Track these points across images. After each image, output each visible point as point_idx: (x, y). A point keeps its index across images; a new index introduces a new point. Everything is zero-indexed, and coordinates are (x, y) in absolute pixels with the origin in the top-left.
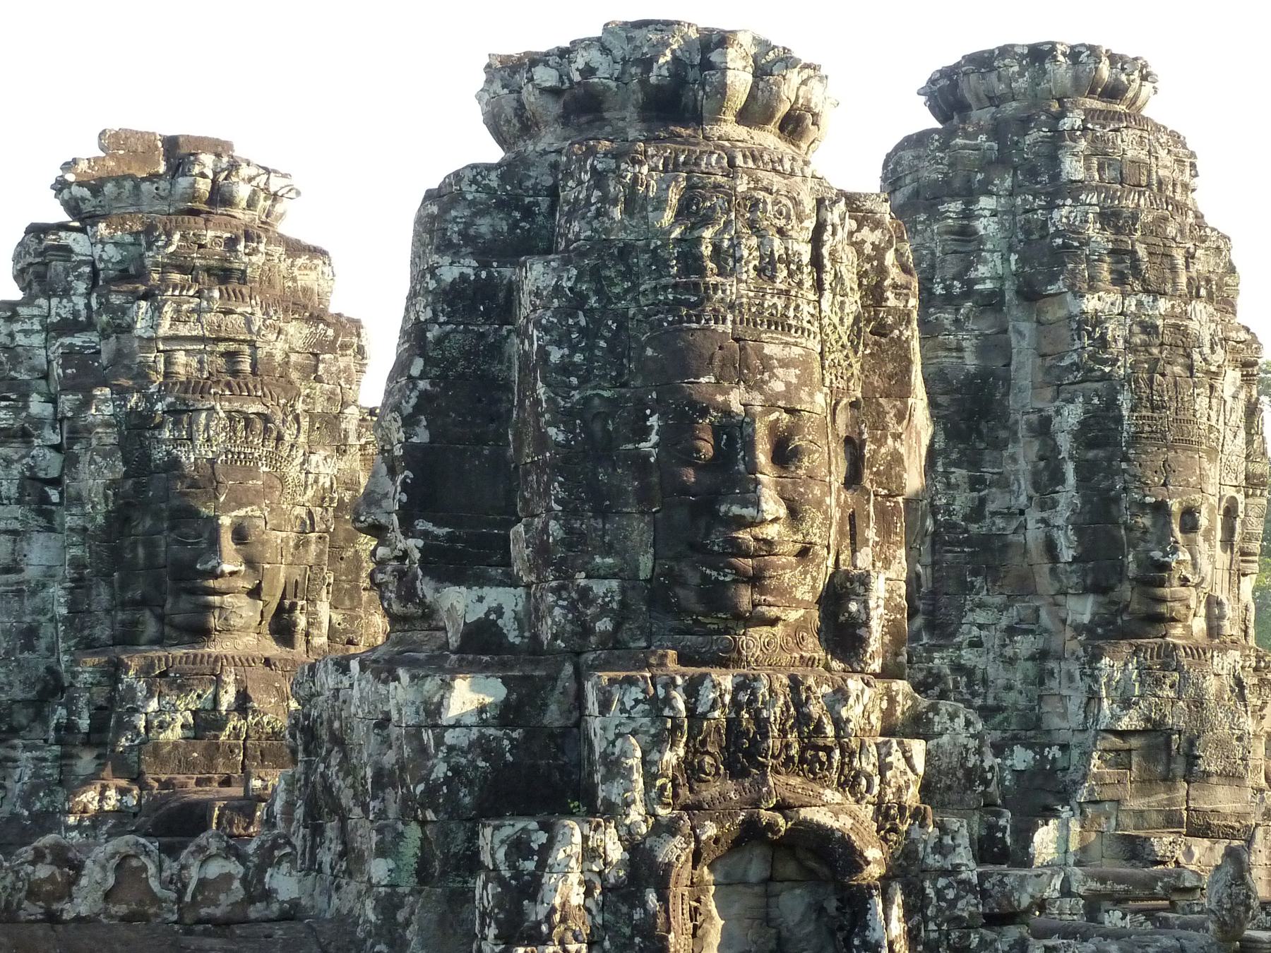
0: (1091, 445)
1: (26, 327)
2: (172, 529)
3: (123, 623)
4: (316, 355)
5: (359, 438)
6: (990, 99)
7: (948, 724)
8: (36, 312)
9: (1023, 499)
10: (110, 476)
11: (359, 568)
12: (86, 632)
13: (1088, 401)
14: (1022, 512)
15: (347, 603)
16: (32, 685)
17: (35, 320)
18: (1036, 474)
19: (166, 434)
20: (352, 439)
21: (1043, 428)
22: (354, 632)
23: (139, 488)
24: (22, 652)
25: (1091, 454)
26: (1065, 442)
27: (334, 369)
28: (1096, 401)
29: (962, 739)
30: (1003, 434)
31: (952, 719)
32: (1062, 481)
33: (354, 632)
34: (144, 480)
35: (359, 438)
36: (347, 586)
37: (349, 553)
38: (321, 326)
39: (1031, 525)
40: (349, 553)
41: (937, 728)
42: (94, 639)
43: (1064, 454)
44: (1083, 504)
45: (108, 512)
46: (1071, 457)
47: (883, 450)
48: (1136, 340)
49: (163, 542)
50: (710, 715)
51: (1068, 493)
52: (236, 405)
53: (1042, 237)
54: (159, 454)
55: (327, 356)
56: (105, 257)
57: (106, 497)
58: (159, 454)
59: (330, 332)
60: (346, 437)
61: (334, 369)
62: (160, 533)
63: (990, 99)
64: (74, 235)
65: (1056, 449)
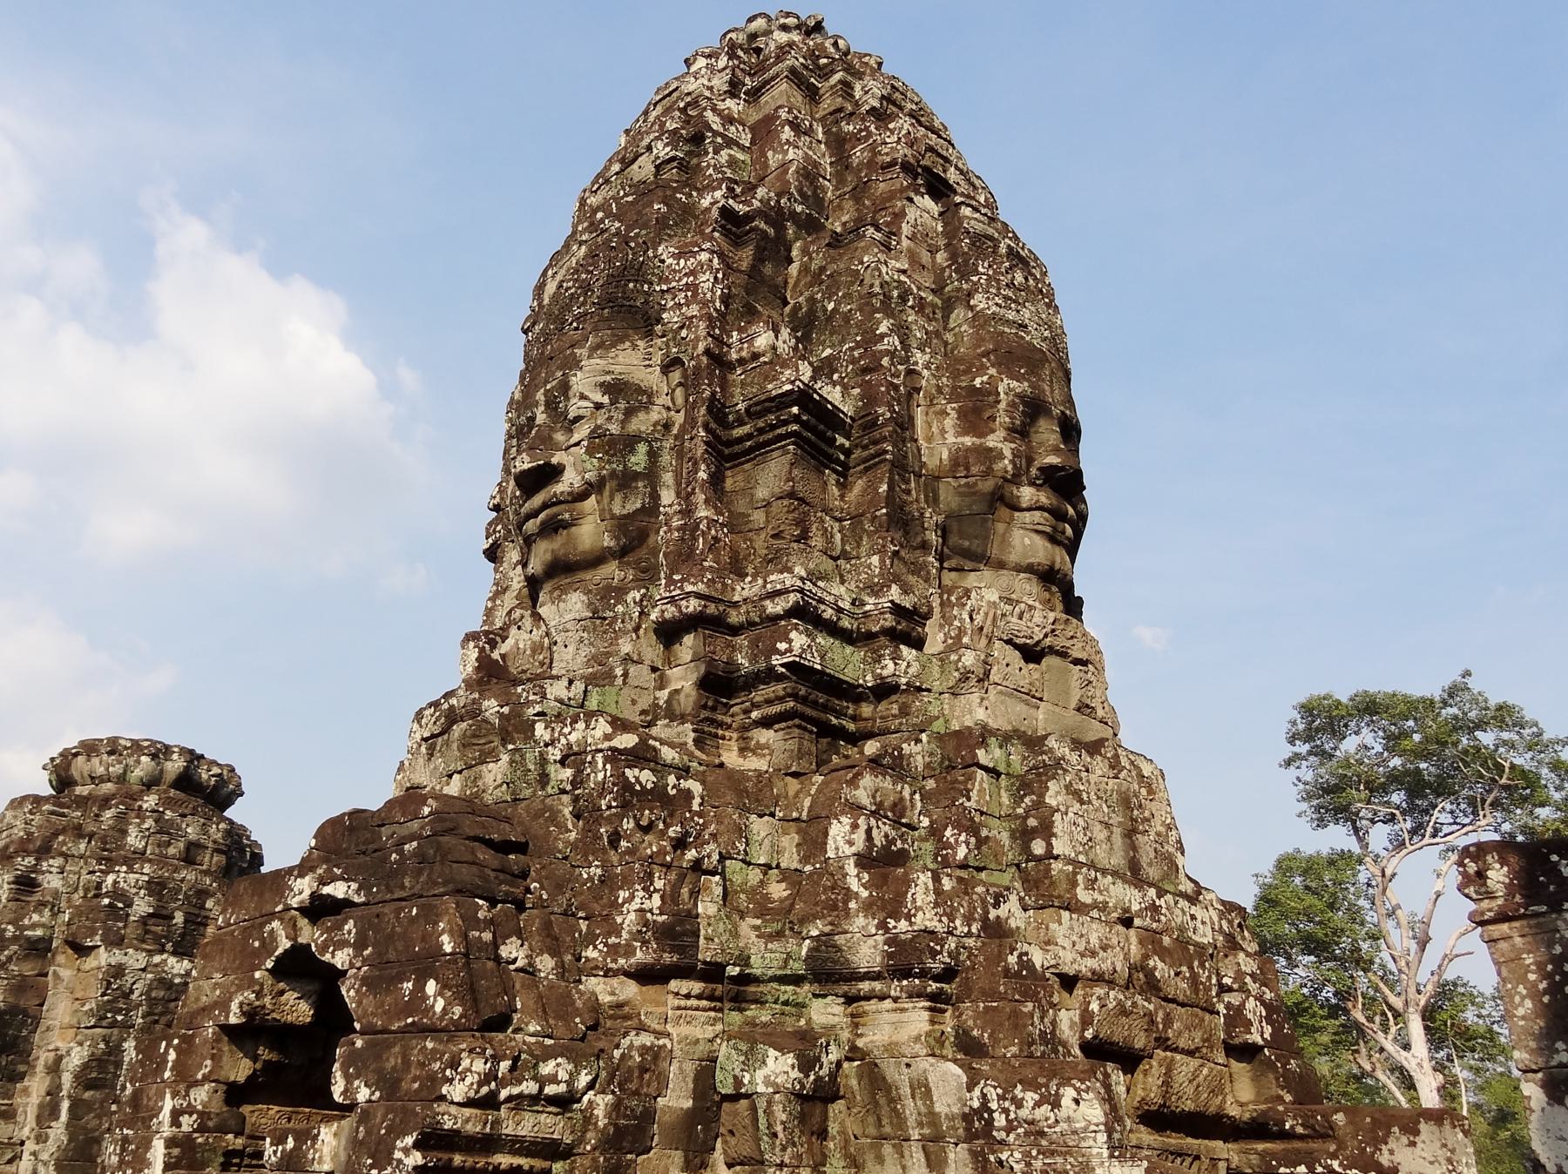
0: (90, 1085)
6: (92, 778)
9: (26, 1131)
13: (94, 1045)
14: (22, 1143)
18: (41, 1106)
21: (55, 1069)
25: (87, 1095)
26: (67, 1079)
28: (102, 1046)
30: (22, 1068)
32: (57, 1119)
39: (26, 1156)
43: (64, 1093)
44: (70, 1141)
46: (69, 1097)
48: (153, 994)
51: (58, 1132)
53: (96, 896)
63: (92, 778)
65: (59, 1087)
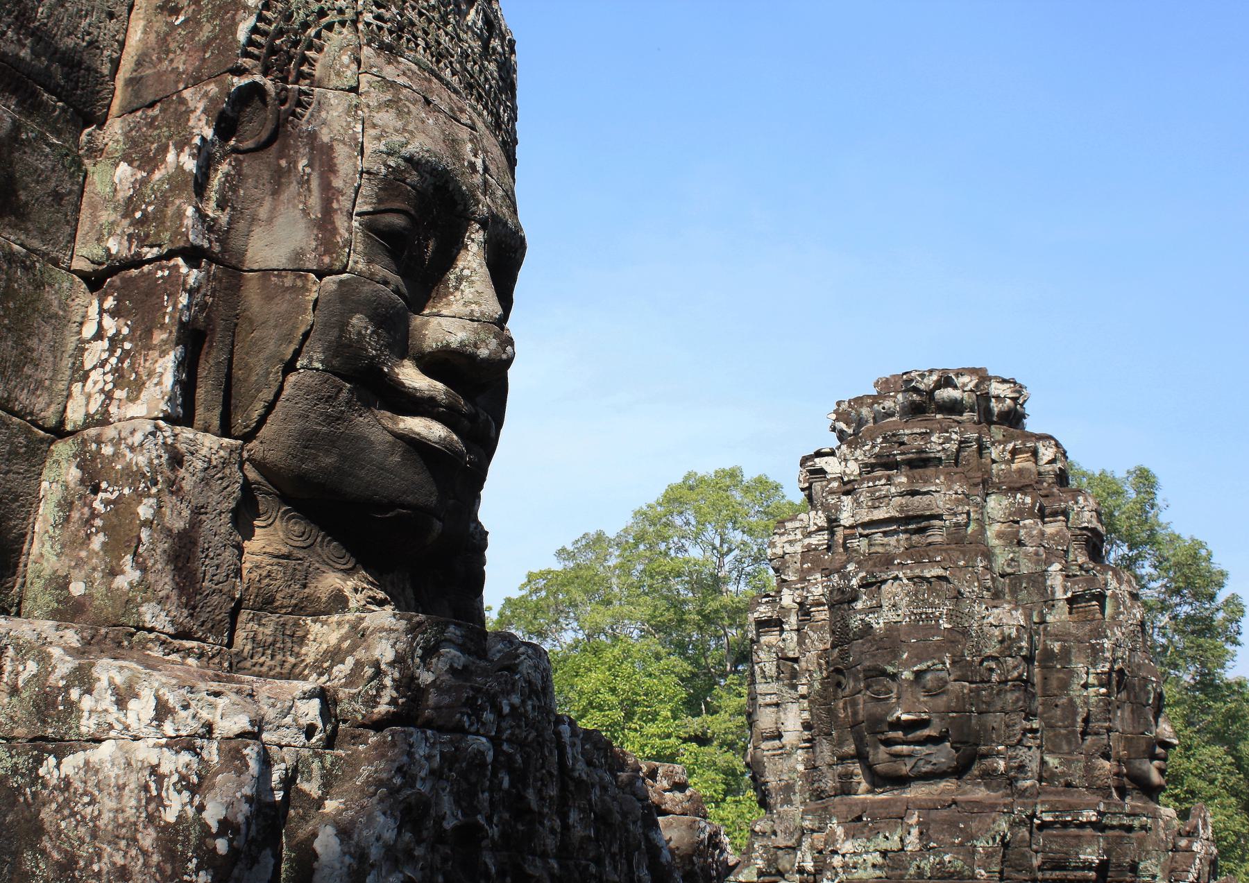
1: (791, 537)
2: (868, 687)
3: (840, 776)
4: (1017, 522)
5: (1065, 592)
7: (114, 714)
8: (797, 524)
10: (822, 647)
11: (1075, 713)
12: (816, 785)
15: (1065, 748)
16: (792, 834)
17: (798, 532)
19: (859, 605)
20: (1059, 594)
22: (1072, 775)
23: (844, 655)
24: (782, 806)
27: (1035, 532)
29: (146, 752)
31: (121, 703)
33: (1072, 775)
34: (846, 647)
35: (1065, 592)
36: (1063, 731)
37: (1063, 701)
38: (1019, 496)
40: (1064, 700)
41: (87, 726)
42: (822, 791)
45: (823, 678)
47: (157, 175)
49: (861, 701)
50: (328, 765)
52: (917, 572)
54: (855, 623)
55: (1027, 522)
56: (848, 471)
57: (820, 665)
58: (855, 623)
59: (1028, 500)
60: (1053, 593)
61: (1035, 532)
62: (859, 692)
64: (826, 458)
